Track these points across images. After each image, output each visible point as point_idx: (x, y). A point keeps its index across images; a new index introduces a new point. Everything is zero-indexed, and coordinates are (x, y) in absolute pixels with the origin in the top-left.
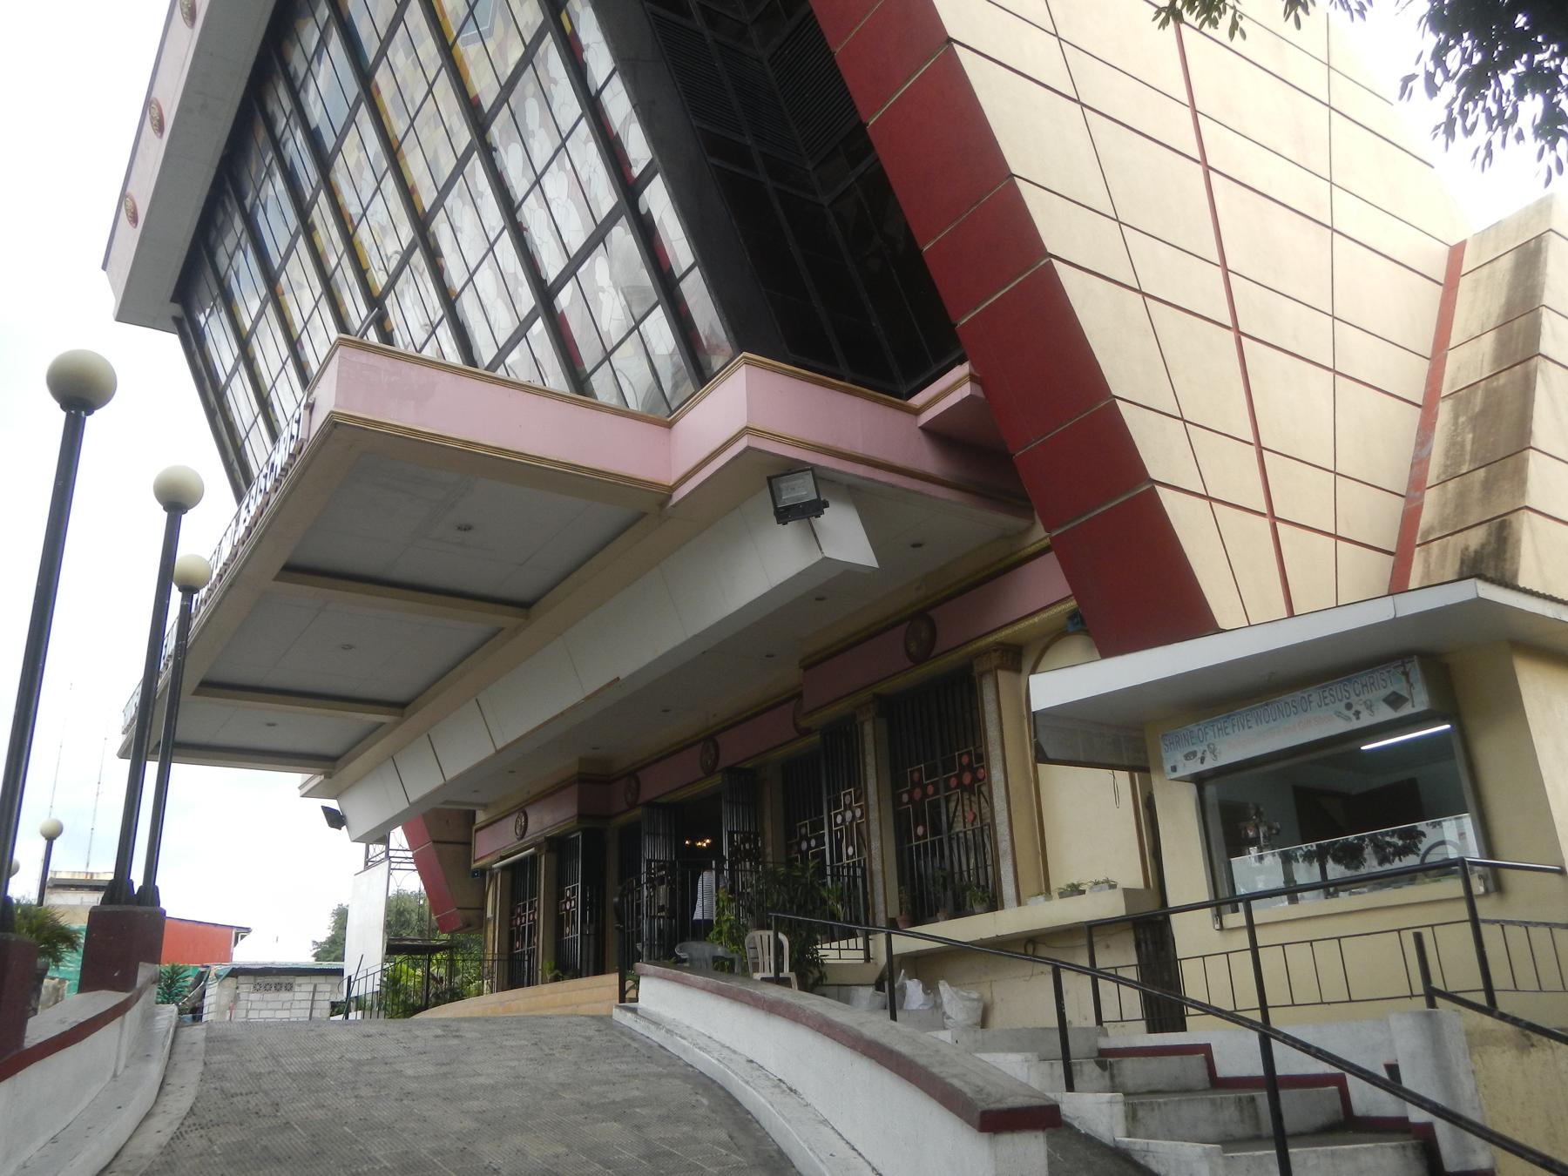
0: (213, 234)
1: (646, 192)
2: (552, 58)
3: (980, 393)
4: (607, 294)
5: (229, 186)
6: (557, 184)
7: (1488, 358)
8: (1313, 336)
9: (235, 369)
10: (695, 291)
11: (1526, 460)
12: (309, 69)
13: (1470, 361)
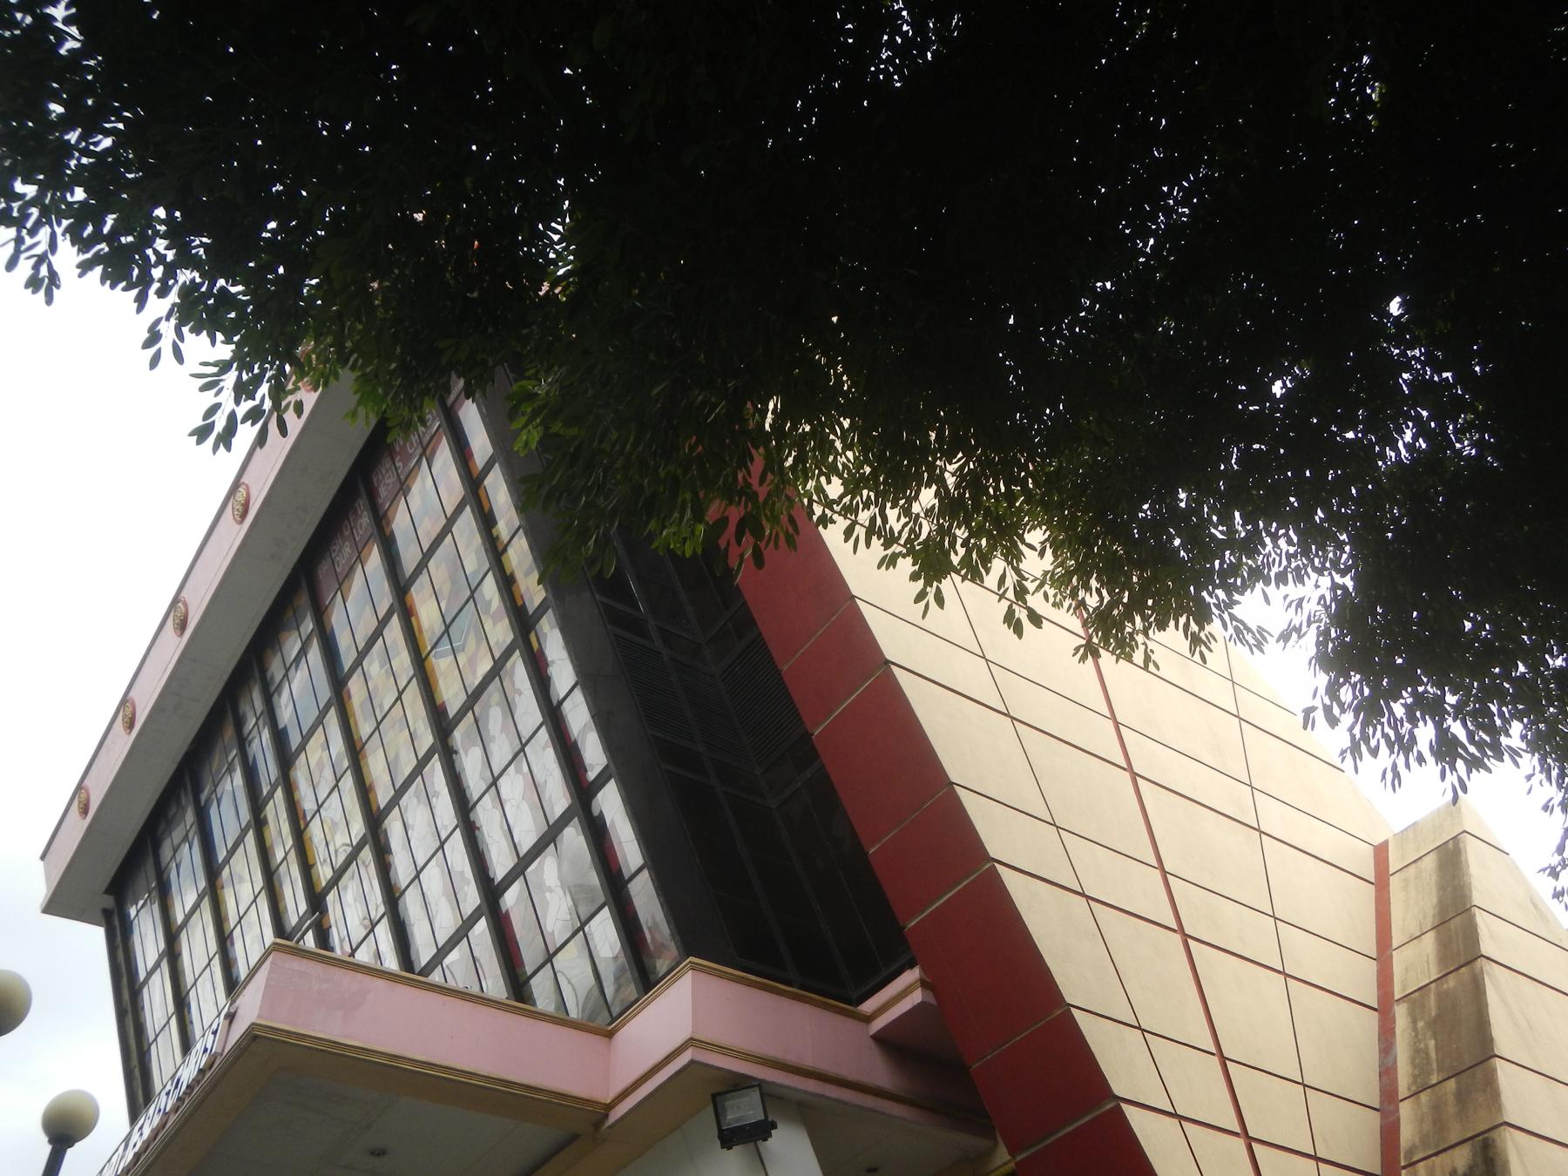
0: (163, 826)
1: (600, 795)
3: (932, 1000)
4: (553, 896)
5: (187, 779)
6: (512, 786)
7: (1433, 959)
8: (1258, 938)
9: (157, 965)
10: (644, 895)
11: (1494, 1070)
12: (286, 675)
13: (1416, 963)
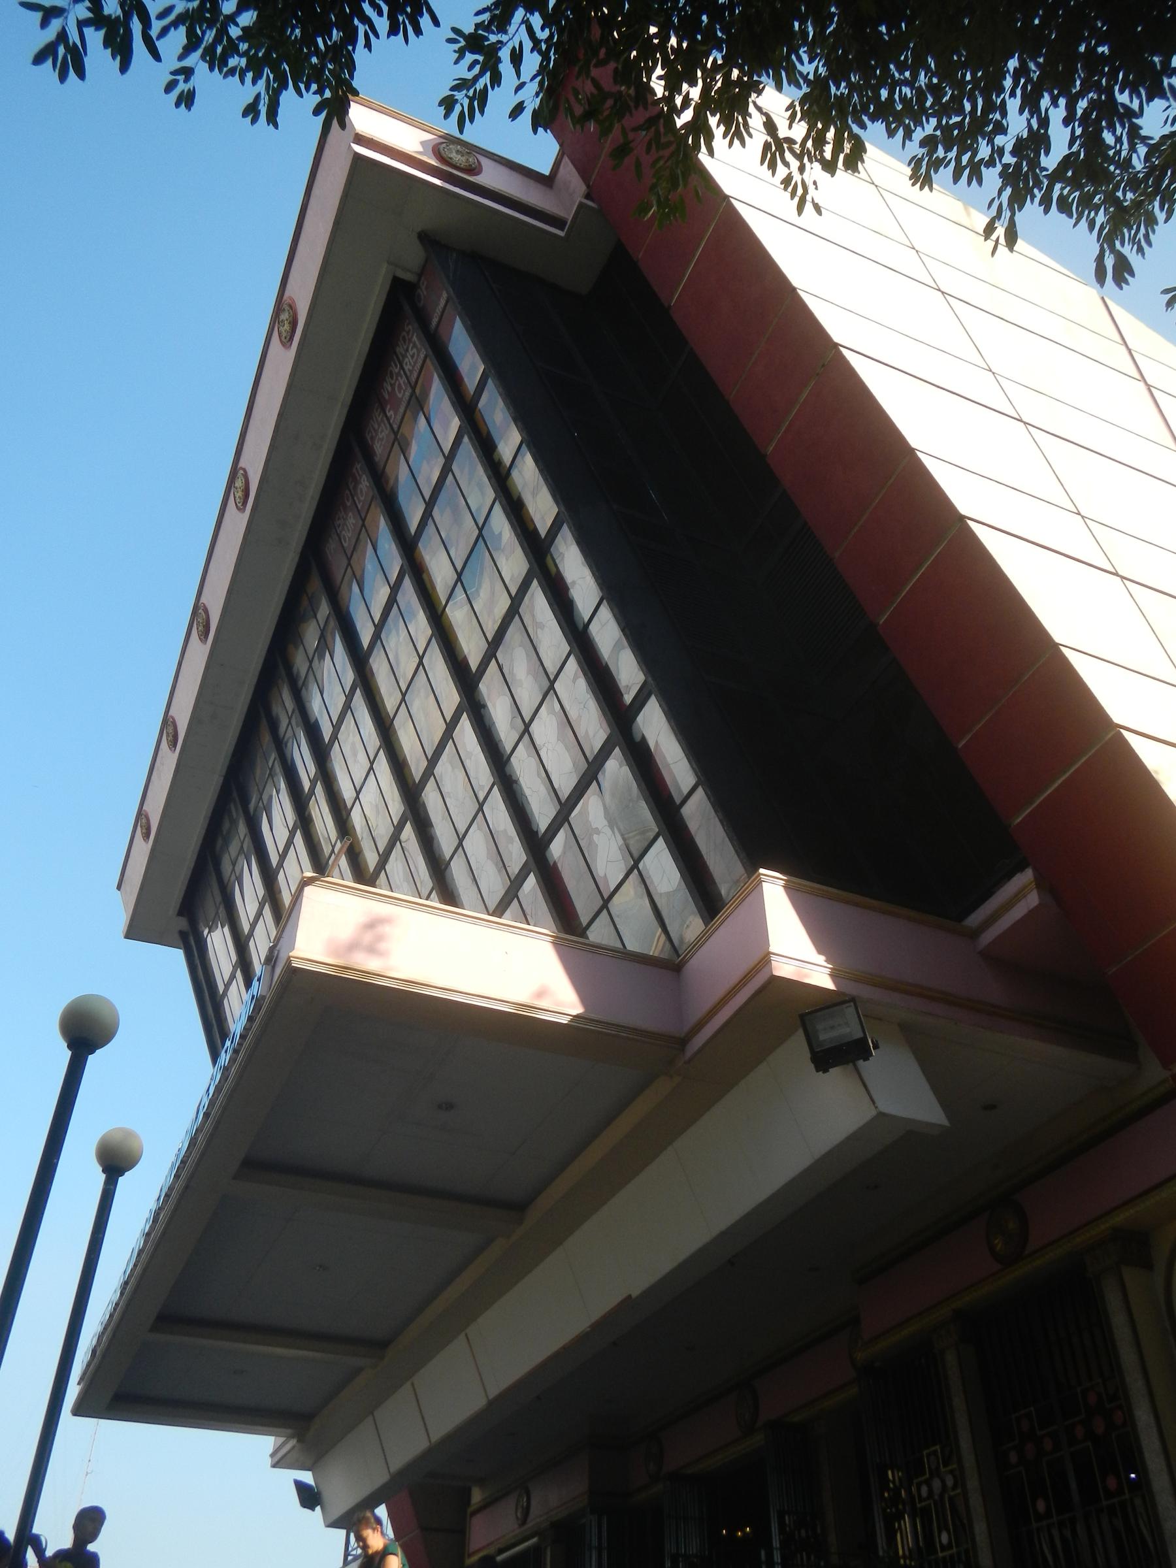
0: (220, 842)
1: (640, 719)
2: (538, 604)
4: (603, 837)
5: (235, 795)
6: (546, 728)
9: (233, 977)
10: (698, 812)
12: (310, 667)
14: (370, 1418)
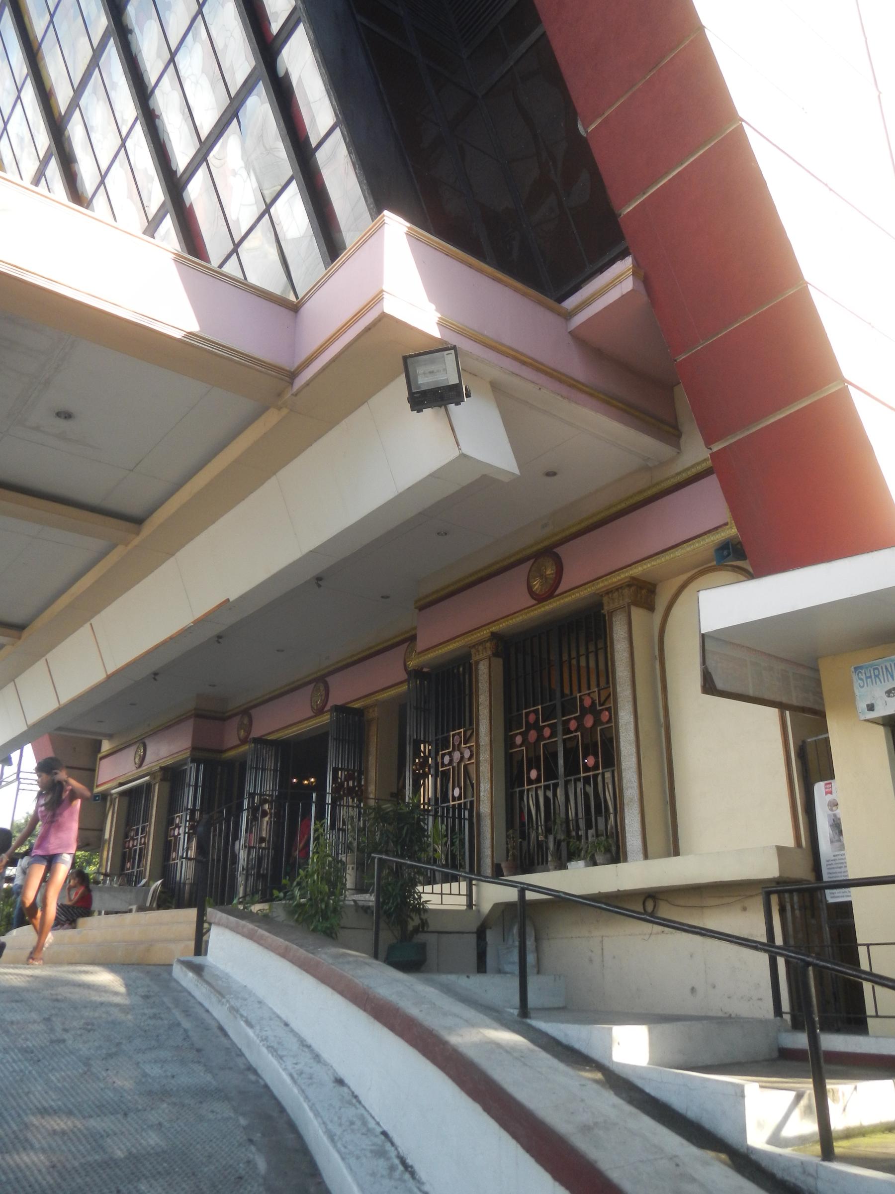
1: (285, 52)
4: (241, 181)
6: (193, 60)
14: (11, 685)
